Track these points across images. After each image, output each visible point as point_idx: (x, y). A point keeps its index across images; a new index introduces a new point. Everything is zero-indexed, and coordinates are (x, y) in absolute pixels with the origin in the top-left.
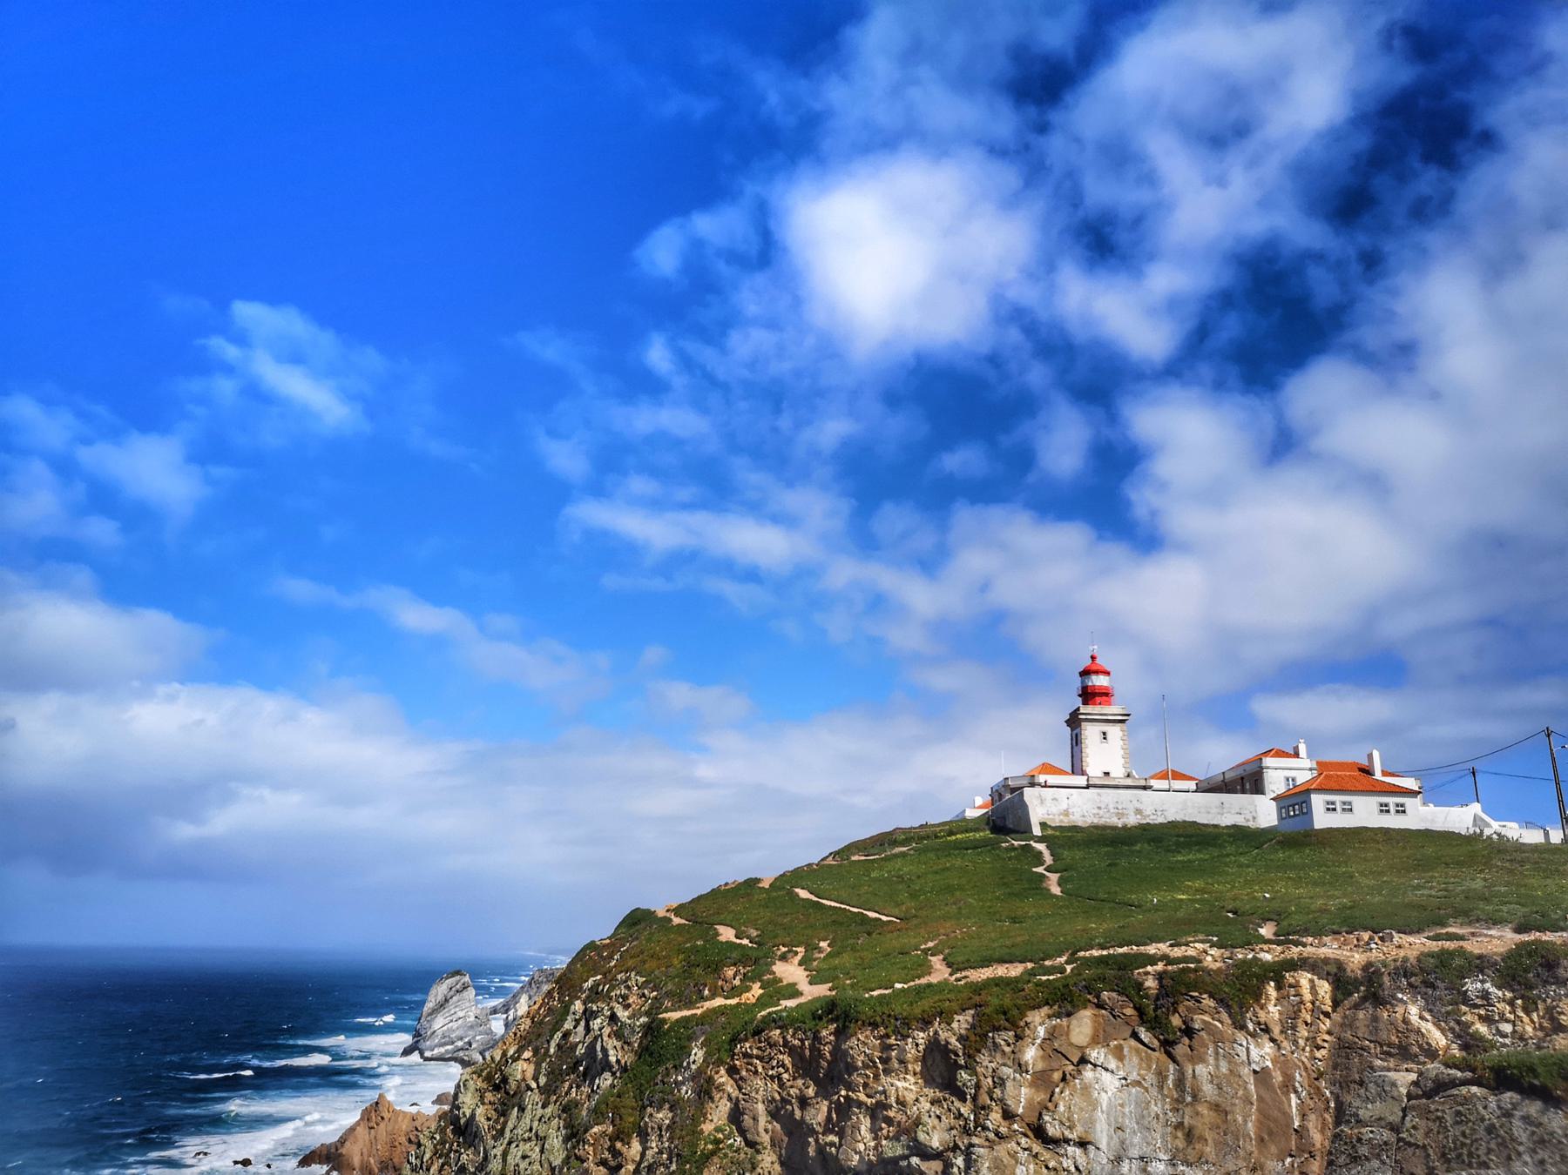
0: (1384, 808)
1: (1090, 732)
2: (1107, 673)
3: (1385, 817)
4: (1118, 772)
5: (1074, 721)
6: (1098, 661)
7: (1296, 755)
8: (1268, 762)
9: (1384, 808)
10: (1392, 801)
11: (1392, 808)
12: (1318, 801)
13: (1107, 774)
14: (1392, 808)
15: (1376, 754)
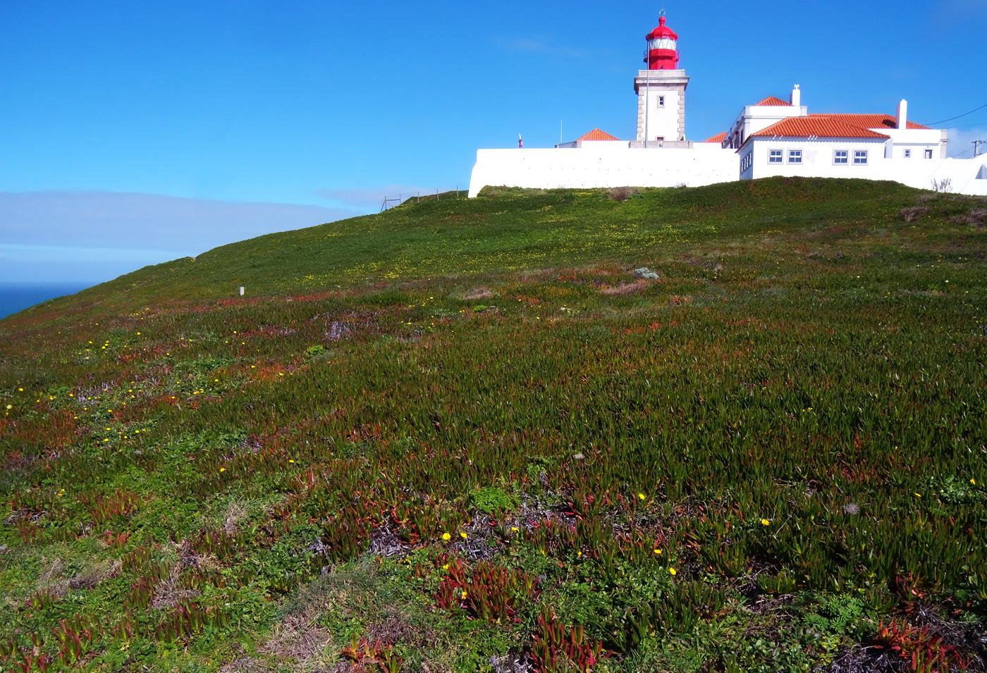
0: (841, 158)
1: (649, 96)
2: (673, 37)
3: (841, 166)
4: (672, 134)
5: (636, 88)
6: (666, 25)
7: (790, 103)
8: (753, 111)
9: (841, 158)
10: (851, 147)
11: (851, 157)
12: (761, 150)
13: (661, 138)
14: (851, 157)
15: (904, 105)
